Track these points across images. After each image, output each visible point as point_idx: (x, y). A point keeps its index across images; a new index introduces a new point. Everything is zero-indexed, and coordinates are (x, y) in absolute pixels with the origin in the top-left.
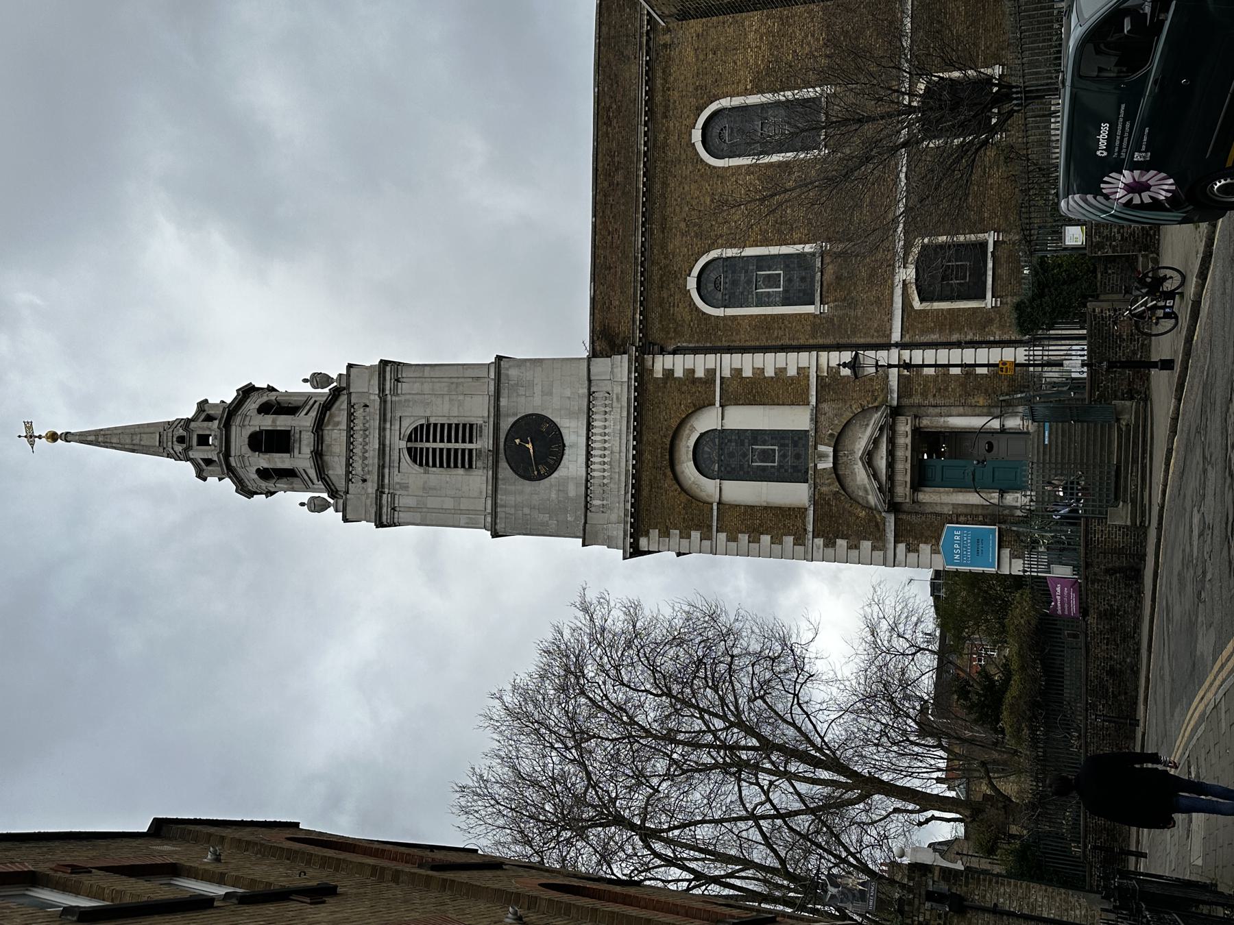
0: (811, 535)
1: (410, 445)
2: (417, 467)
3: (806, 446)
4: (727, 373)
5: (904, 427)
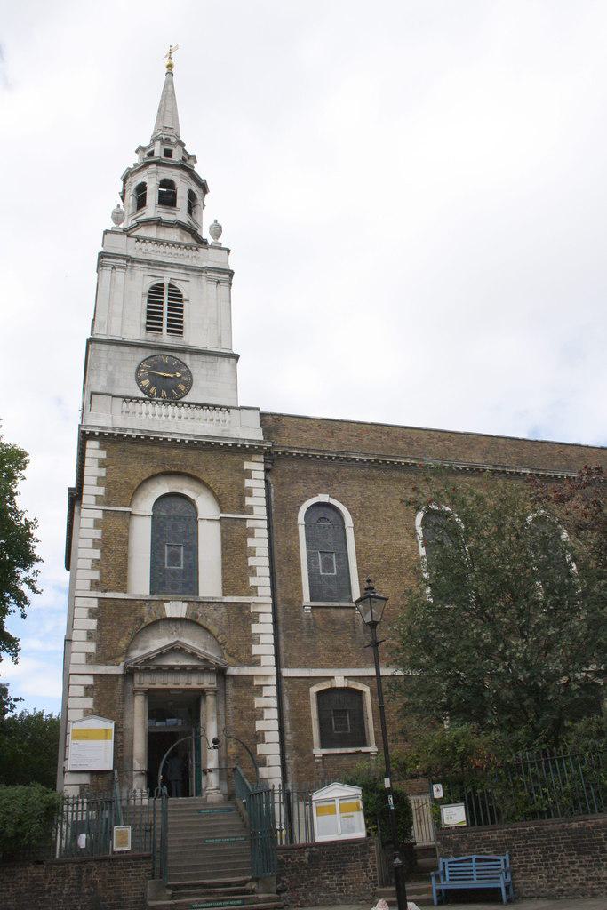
0: (101, 595)
1: (166, 286)
2: (148, 289)
4: (249, 524)
5: (208, 682)
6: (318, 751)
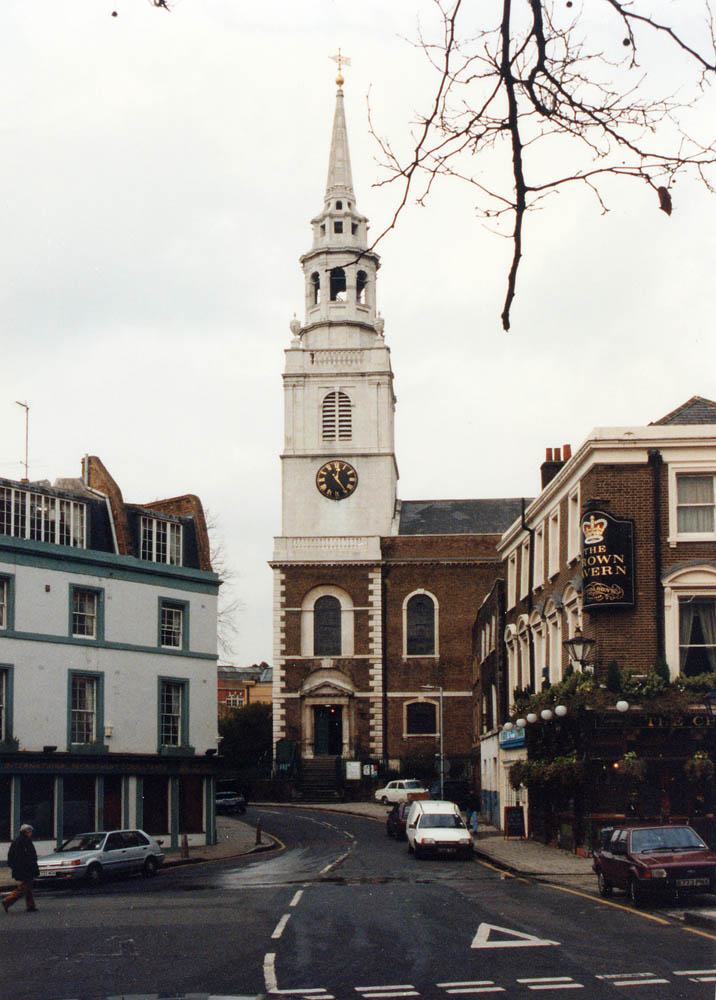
3: (334, 654)
4: (370, 613)
5: (343, 701)
6: (405, 735)
